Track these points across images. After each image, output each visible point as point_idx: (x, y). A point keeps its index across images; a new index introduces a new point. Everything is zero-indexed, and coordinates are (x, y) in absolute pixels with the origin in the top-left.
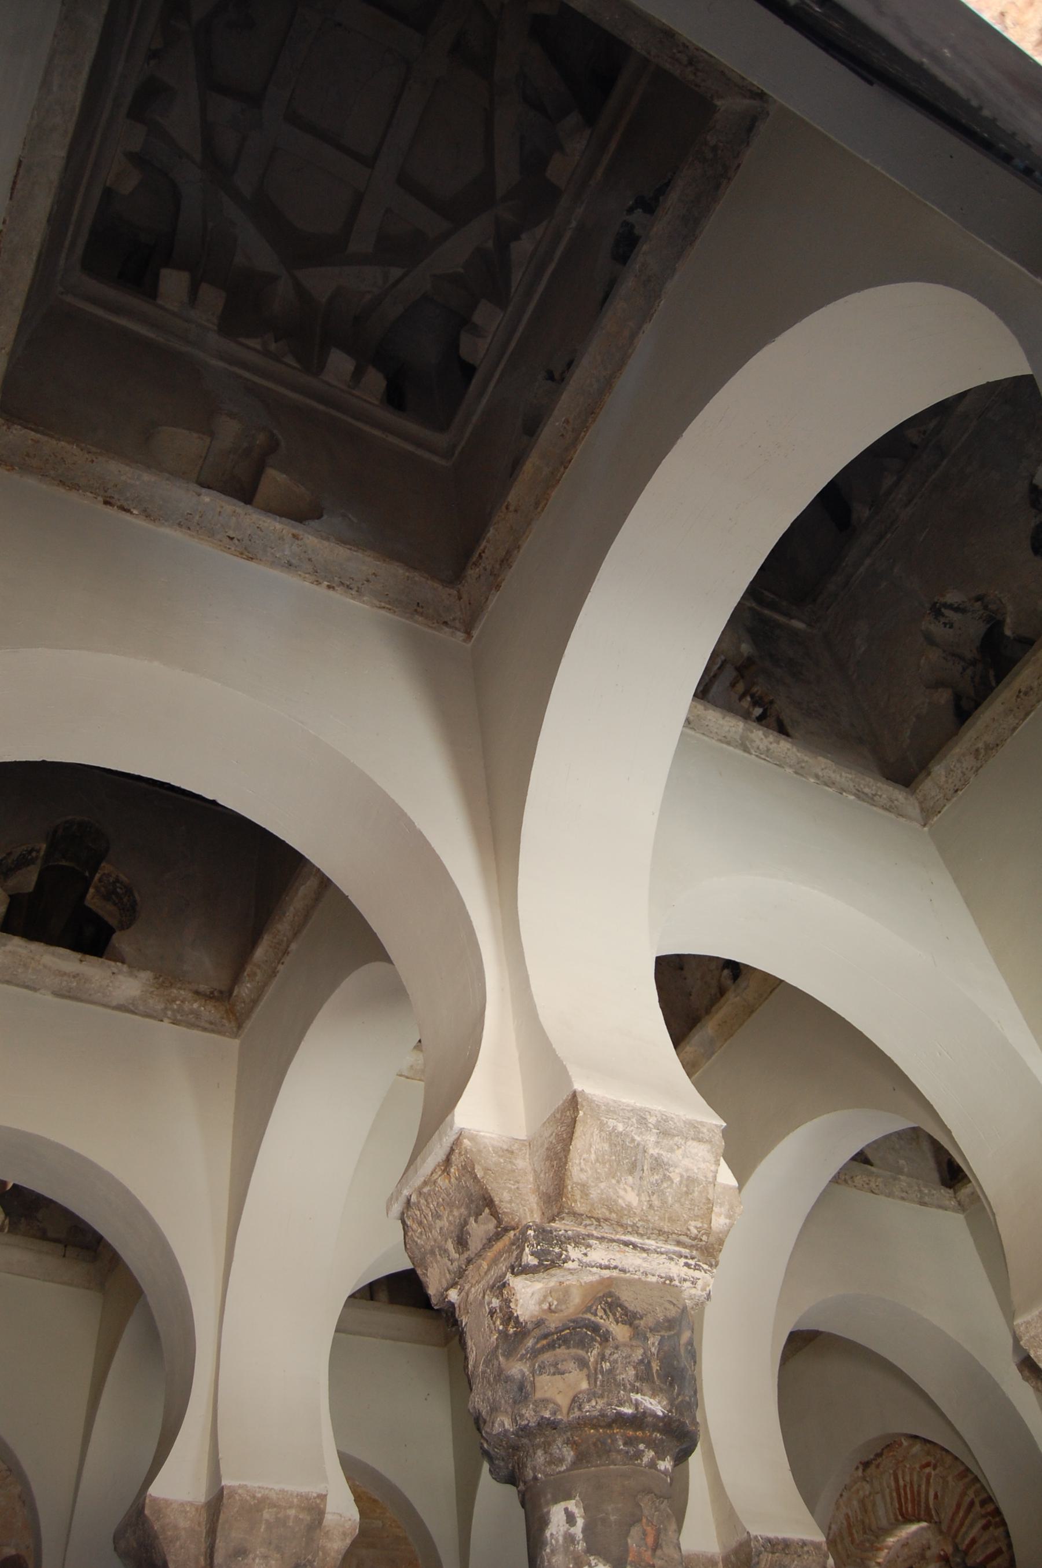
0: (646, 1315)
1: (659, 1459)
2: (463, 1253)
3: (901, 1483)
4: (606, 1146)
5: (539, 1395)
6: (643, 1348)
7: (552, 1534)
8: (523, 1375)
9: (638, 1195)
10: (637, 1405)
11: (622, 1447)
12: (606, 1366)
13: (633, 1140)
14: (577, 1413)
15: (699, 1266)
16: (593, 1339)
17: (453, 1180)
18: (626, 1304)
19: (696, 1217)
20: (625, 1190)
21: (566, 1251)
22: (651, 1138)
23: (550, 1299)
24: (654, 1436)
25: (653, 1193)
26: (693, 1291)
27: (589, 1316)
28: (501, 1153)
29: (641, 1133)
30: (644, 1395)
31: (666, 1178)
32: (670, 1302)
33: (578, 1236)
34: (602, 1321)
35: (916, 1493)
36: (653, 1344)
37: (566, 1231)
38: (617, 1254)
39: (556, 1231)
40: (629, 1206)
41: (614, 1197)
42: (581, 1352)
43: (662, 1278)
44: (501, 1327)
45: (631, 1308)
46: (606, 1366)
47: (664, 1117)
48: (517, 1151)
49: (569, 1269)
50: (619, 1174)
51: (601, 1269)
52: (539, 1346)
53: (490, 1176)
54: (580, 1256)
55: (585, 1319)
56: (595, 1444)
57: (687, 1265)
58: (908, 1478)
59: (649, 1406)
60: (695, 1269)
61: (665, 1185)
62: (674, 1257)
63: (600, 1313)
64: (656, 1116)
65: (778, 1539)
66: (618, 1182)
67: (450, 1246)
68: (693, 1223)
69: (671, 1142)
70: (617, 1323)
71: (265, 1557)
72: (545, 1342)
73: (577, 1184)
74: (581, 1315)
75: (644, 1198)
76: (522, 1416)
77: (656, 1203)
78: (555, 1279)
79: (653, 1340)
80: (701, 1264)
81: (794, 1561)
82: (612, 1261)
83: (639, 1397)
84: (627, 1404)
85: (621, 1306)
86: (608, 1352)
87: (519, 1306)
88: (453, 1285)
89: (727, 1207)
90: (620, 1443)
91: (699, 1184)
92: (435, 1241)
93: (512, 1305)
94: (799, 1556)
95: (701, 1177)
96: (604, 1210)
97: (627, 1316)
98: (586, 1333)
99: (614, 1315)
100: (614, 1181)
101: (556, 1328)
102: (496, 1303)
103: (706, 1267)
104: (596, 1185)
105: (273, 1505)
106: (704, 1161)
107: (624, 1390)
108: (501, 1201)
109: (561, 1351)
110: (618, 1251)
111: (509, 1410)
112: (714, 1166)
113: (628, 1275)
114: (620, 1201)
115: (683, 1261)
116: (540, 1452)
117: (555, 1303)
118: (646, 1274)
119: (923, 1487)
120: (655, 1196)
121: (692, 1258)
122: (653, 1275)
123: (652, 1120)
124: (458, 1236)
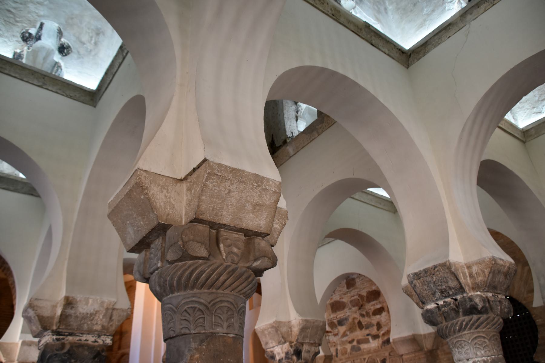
65: (420, 271)
71: (272, 343)
81: (433, 277)
94: (434, 274)
105: (265, 330)
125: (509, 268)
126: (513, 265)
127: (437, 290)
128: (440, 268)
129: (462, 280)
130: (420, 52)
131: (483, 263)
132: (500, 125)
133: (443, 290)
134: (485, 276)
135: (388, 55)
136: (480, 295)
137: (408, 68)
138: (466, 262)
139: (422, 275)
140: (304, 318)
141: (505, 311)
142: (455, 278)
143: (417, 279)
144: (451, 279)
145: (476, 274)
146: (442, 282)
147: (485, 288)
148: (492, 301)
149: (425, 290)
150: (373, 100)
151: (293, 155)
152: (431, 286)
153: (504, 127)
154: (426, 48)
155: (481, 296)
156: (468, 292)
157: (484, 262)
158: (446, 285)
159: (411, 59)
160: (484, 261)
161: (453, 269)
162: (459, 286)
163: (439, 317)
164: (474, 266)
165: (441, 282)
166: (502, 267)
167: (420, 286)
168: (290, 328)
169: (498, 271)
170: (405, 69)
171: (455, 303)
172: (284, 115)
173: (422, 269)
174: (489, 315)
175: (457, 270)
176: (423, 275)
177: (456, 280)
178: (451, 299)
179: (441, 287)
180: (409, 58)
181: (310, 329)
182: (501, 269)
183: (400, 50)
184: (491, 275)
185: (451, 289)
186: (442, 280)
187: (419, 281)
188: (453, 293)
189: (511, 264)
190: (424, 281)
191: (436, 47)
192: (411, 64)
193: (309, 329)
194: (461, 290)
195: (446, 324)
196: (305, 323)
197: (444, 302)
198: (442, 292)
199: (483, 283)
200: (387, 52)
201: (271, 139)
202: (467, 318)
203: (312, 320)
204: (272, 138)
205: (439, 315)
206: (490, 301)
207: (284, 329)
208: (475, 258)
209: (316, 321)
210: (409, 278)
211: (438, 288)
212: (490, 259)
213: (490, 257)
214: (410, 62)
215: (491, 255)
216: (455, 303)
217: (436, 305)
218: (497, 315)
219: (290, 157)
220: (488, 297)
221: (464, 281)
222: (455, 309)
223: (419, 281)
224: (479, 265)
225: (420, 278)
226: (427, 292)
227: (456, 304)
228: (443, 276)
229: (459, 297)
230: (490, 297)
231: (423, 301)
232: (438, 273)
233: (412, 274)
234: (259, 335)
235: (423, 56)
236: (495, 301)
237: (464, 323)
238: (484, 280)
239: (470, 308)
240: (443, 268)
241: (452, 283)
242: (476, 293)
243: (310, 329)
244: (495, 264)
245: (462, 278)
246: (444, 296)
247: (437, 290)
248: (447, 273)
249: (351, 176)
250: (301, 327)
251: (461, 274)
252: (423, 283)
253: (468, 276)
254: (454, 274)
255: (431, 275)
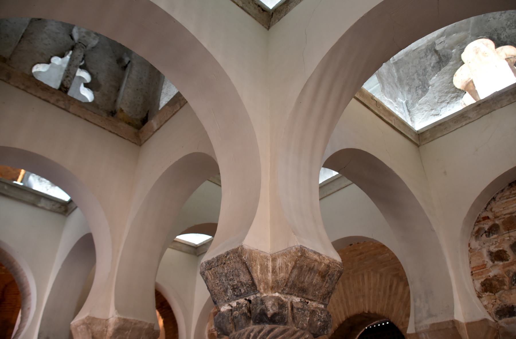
65: (214, 258)
81: (224, 268)
94: (225, 264)
105: (78, 326)
125: (328, 266)
126: (337, 264)
127: (229, 286)
128: (232, 255)
129: (257, 274)
130: (282, 10)
131: (288, 255)
132: (356, 96)
133: (235, 287)
134: (287, 272)
135: (242, 8)
136: (278, 297)
137: (268, 29)
138: (271, 253)
139: (213, 264)
140: (122, 317)
141: (317, 325)
142: (247, 271)
143: (208, 270)
144: (243, 271)
145: (279, 269)
146: (234, 275)
147: (285, 288)
148: (298, 309)
149: (217, 285)
150: (194, 42)
151: (156, 130)
152: (223, 280)
153: (393, 124)
154: (288, 7)
155: (278, 299)
156: (262, 291)
157: (290, 253)
158: (238, 280)
159: (273, 19)
160: (290, 251)
161: (245, 258)
162: (251, 282)
163: (230, 323)
164: (279, 258)
165: (233, 275)
166: (316, 264)
167: (212, 280)
168: (107, 327)
169: (308, 268)
170: (265, 30)
171: (248, 306)
172: (162, 90)
173: (215, 256)
174: (287, 327)
175: (252, 259)
176: (215, 264)
177: (247, 273)
178: (244, 300)
179: (233, 282)
180: (271, 18)
181: (130, 331)
182: (314, 265)
183: (259, 6)
184: (295, 272)
185: (243, 286)
186: (233, 273)
187: (211, 273)
188: (245, 292)
189: (334, 261)
190: (215, 273)
191: (298, 4)
192: (272, 25)
193: (129, 330)
194: (252, 288)
196: (122, 323)
197: (238, 303)
198: (234, 289)
199: (283, 281)
200: (241, 4)
201: (145, 115)
202: (257, 328)
203: (134, 320)
204: (147, 114)
205: (230, 322)
206: (295, 307)
207: (97, 328)
208: (281, 247)
209: (140, 322)
210: (201, 268)
211: (230, 283)
212: (297, 249)
213: (297, 246)
214: (271, 23)
215: (299, 244)
216: (248, 306)
217: (230, 308)
218: (302, 329)
219: (154, 132)
220: (293, 302)
221: (260, 276)
222: (246, 313)
223: (210, 271)
224: (285, 257)
225: (211, 269)
226: (219, 288)
227: (250, 307)
228: (234, 266)
229: (252, 298)
230: (297, 302)
231: (215, 300)
232: (229, 262)
233: (205, 263)
234: (73, 332)
235: (284, 16)
236: (301, 309)
237: (252, 334)
238: (286, 277)
239: (259, 314)
240: (234, 255)
241: (244, 278)
242: (274, 295)
243: (130, 331)
244: (301, 256)
245: (259, 271)
246: (236, 295)
247: (229, 286)
248: (238, 262)
249: (195, 151)
250: (116, 327)
251: (259, 267)
252: (215, 275)
253: (271, 271)
254: (246, 264)
255: (222, 265)
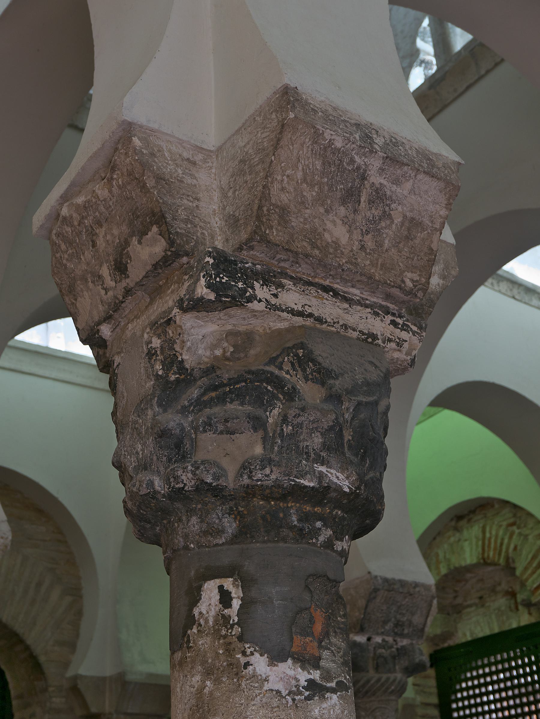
0: (342, 375)
1: (337, 539)
2: (120, 281)
3: (488, 535)
4: (318, 165)
5: (200, 456)
6: (336, 413)
7: (201, 613)
8: (183, 429)
9: (350, 231)
10: (321, 476)
11: (296, 523)
12: (288, 429)
13: (352, 161)
14: (246, 481)
15: (408, 326)
16: (274, 397)
17: (115, 190)
18: (320, 359)
19: (412, 268)
20: (334, 222)
21: (253, 288)
22: (375, 163)
23: (226, 344)
24: (334, 513)
25: (367, 232)
26: (396, 355)
27: (271, 368)
28: (179, 162)
29: (364, 154)
30: (331, 468)
31: (386, 215)
32: (371, 363)
33: (269, 273)
34: (288, 377)
35: (498, 544)
36: (348, 409)
37: (254, 265)
38: (314, 300)
39: (242, 262)
40: (336, 244)
41: (320, 230)
42: (259, 412)
43: (363, 334)
44: (160, 373)
45: (326, 364)
46: (288, 429)
47: (394, 140)
48: (200, 163)
49: (253, 311)
50: (329, 202)
51: (293, 315)
52: (206, 398)
53: (163, 187)
54: (269, 297)
55: (268, 372)
56: (263, 518)
57: (393, 323)
58: (494, 532)
59: (336, 480)
60: (402, 329)
61: (383, 224)
62: (380, 312)
63: (287, 367)
64: (384, 137)
66: (327, 211)
67: (105, 271)
68: (409, 275)
69: (399, 171)
70: (306, 379)
72: (213, 394)
73: (276, 206)
74: (261, 367)
75: (357, 236)
76: (177, 479)
77: (370, 244)
78: (233, 321)
79: (348, 406)
80: (409, 324)
82: (307, 307)
83: (323, 469)
84: (308, 476)
85: (313, 361)
86: (292, 413)
87: (185, 349)
88: (107, 318)
89: (442, 266)
90: (294, 518)
91: (423, 230)
92: (88, 264)
93: (177, 347)
95: (426, 221)
96: (305, 244)
97: (319, 373)
98: (266, 388)
99: (304, 370)
100: (322, 210)
101: (230, 379)
102: (156, 343)
103: (415, 328)
104: (299, 211)
106: (434, 203)
107: (307, 460)
108: (174, 219)
109: (233, 407)
110: (315, 297)
111: (162, 469)
112: (444, 209)
113: (324, 326)
114: (327, 236)
115: (390, 318)
116: (194, 520)
117: (232, 349)
118: (346, 328)
119: (506, 541)
120: (370, 236)
121: (400, 317)
122: (354, 330)
123: (379, 141)
124: (115, 260)
127: (393, 619)
133: (400, 623)
165: (407, 611)
195: (377, 676)
197: (383, 640)
198: (396, 625)
233: (381, 579)
